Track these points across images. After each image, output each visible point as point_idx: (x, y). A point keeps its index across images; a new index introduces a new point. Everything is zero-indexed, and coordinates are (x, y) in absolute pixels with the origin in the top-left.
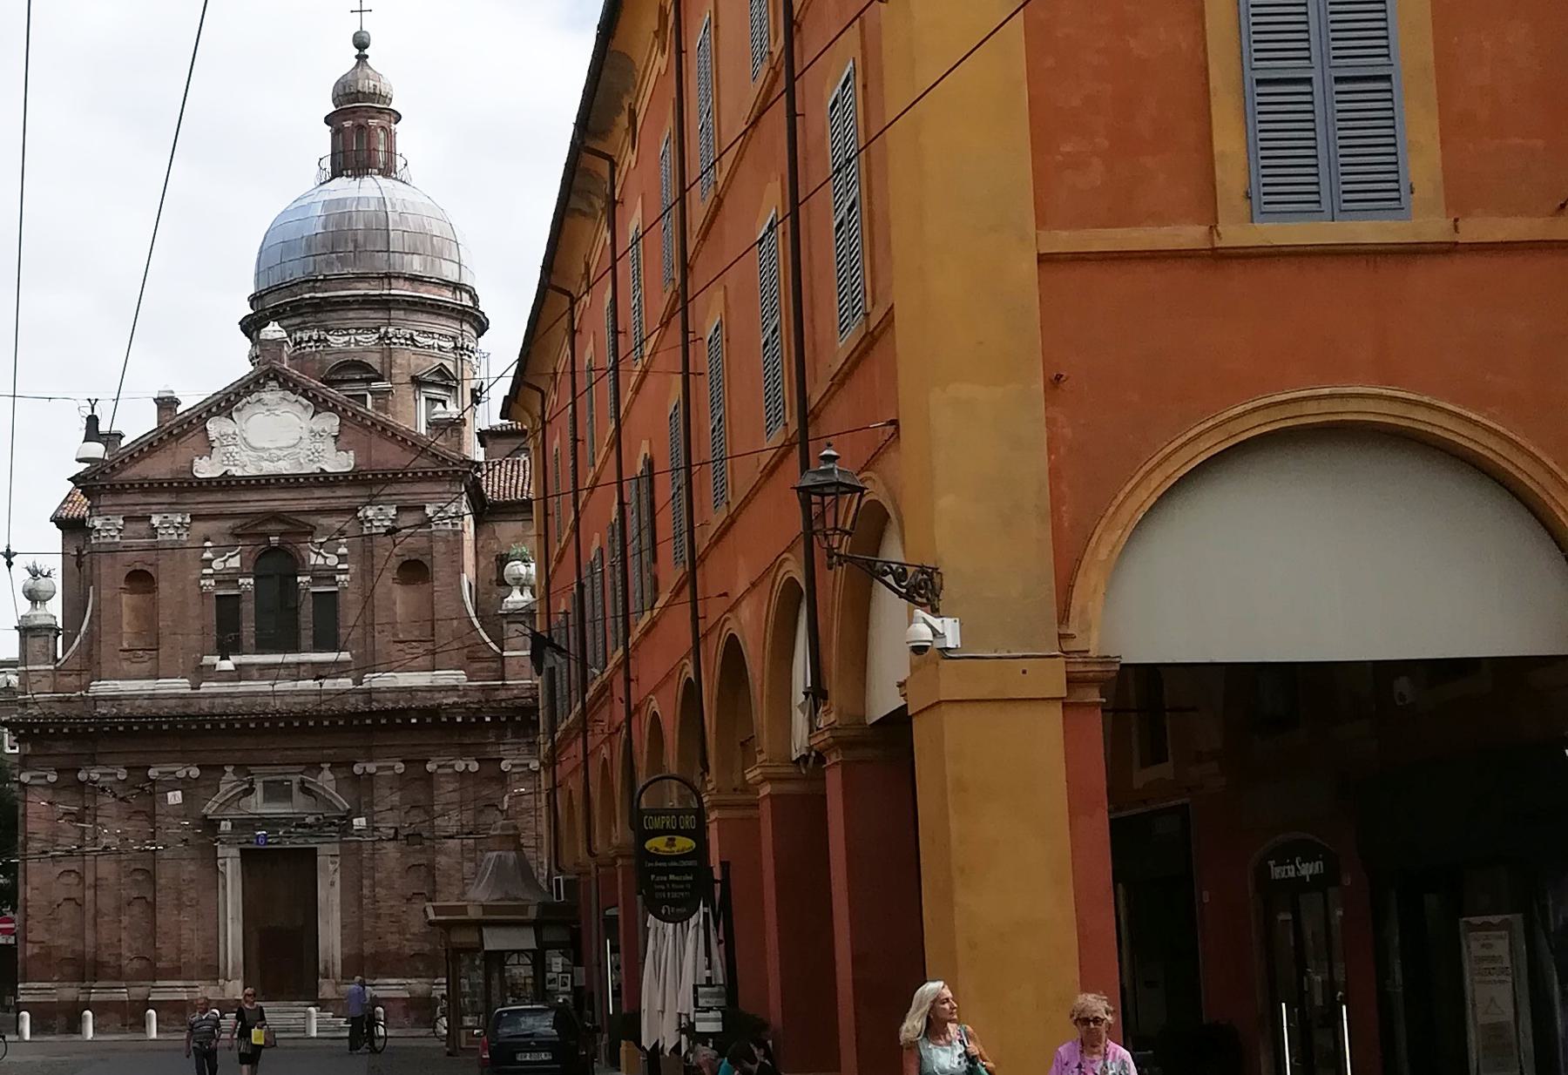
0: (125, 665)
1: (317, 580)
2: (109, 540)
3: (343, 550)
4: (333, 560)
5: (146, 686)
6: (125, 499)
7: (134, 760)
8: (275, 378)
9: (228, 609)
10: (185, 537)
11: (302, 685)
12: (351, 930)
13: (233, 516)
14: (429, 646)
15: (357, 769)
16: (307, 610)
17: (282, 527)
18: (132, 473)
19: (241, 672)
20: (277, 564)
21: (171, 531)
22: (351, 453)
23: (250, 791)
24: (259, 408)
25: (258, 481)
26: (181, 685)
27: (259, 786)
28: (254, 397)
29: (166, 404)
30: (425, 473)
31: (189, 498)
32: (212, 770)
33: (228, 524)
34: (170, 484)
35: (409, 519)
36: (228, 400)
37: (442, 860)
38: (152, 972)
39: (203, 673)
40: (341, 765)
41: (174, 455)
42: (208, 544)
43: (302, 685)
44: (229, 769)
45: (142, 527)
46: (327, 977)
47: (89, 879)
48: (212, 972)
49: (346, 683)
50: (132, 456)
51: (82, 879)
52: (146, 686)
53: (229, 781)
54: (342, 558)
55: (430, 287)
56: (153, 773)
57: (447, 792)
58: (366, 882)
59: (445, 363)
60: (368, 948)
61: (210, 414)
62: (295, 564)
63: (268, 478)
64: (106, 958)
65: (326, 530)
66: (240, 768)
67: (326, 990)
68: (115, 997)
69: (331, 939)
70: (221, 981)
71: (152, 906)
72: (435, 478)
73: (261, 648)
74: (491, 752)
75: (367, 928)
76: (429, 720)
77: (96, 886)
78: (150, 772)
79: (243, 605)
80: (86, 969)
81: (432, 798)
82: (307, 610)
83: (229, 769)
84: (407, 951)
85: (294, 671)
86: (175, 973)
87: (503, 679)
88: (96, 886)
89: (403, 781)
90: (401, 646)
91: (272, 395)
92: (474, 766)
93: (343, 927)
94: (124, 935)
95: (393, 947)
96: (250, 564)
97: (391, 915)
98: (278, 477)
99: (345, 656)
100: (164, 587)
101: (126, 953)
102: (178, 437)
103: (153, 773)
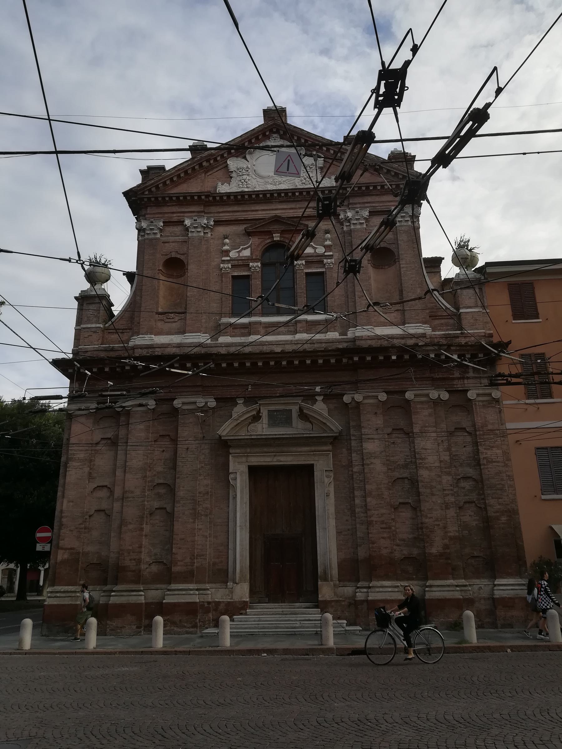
0: (160, 325)
1: (309, 263)
3: (328, 243)
4: (321, 250)
5: (176, 339)
7: (162, 393)
8: (277, 132)
9: (241, 283)
10: (209, 235)
11: (299, 336)
12: (348, 537)
13: (246, 221)
15: (346, 399)
16: (301, 283)
17: (283, 228)
19: (248, 329)
20: (279, 256)
23: (257, 418)
25: (265, 195)
26: (203, 338)
27: (264, 413)
31: (213, 209)
33: (241, 228)
34: (199, 197)
37: (424, 473)
38: (167, 576)
39: (219, 330)
44: (240, 401)
45: (178, 229)
46: (325, 579)
47: (118, 492)
48: (222, 575)
49: (333, 335)
50: (171, 179)
51: (112, 492)
52: (176, 339)
53: (240, 410)
54: (328, 248)
56: (177, 403)
57: (423, 417)
58: (357, 493)
60: (362, 553)
63: (272, 192)
66: (250, 400)
67: (326, 592)
68: (133, 599)
69: (328, 547)
70: (230, 584)
71: (170, 516)
73: (263, 314)
74: (458, 385)
75: (359, 534)
77: (123, 499)
78: (175, 402)
79: (253, 282)
80: (109, 573)
81: (411, 424)
82: (301, 283)
83: (240, 401)
84: (398, 555)
85: (292, 329)
86: (188, 576)
87: (461, 328)
88: (123, 499)
89: (385, 408)
92: (445, 396)
93: (339, 533)
94: (145, 542)
95: (385, 552)
96: (258, 254)
97: (383, 522)
98: (279, 192)
100: (192, 269)
101: (145, 557)
103: (177, 403)
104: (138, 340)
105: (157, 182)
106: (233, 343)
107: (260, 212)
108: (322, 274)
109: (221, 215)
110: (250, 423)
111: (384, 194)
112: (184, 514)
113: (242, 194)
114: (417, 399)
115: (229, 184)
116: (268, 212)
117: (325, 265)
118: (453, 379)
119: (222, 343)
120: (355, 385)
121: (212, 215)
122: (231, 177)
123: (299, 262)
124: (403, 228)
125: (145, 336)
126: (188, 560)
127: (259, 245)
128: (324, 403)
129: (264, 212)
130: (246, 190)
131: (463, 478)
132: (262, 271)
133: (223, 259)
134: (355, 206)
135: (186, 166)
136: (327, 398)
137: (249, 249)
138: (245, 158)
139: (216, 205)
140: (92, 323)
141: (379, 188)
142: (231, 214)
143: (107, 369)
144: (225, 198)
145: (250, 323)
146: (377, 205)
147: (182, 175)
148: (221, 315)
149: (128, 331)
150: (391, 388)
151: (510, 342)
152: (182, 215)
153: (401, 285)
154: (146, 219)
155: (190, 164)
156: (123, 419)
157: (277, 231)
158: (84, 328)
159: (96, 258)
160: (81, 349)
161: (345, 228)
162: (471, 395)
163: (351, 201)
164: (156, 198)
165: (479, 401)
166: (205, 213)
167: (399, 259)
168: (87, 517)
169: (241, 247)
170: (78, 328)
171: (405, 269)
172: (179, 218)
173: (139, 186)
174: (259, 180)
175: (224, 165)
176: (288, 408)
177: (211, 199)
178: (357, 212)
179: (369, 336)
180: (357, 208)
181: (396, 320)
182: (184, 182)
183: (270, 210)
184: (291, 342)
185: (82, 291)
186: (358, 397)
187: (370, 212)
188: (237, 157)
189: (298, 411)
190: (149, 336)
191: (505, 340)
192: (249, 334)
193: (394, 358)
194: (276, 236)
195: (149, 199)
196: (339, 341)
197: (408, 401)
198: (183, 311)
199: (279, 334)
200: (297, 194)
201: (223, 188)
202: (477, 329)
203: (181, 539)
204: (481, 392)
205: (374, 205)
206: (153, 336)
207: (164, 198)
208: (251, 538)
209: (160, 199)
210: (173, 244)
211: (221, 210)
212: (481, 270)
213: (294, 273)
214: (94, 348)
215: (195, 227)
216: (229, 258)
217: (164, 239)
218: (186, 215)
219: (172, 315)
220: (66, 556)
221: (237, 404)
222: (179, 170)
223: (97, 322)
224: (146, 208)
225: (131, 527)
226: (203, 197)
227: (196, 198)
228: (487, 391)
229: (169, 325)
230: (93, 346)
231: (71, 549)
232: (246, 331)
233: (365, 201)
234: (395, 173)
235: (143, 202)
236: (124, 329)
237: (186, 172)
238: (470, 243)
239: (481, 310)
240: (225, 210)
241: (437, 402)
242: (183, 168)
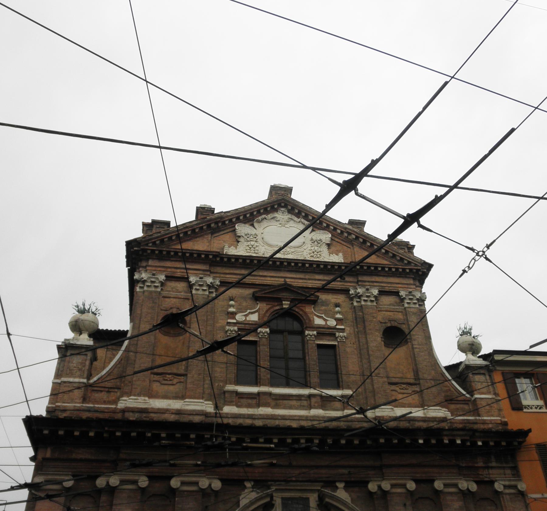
0: (156, 386)
2: (153, 289)
3: (339, 316)
4: (332, 323)
8: (285, 206)
14: (417, 389)
15: (372, 487)
16: (313, 356)
19: (257, 399)
21: (205, 288)
22: (341, 255)
24: (273, 222)
28: (270, 216)
31: (219, 269)
32: (234, 484)
33: (248, 292)
34: (207, 256)
35: (387, 300)
36: (252, 214)
40: (355, 484)
41: (210, 242)
42: (232, 303)
43: (314, 412)
44: (248, 485)
45: (181, 286)
52: (176, 405)
56: (175, 483)
61: (238, 220)
62: (303, 323)
65: (326, 303)
66: (260, 484)
73: (272, 385)
74: (485, 475)
76: (433, 441)
82: (313, 356)
83: (248, 485)
85: (305, 403)
90: (393, 387)
91: (282, 215)
92: (474, 487)
99: (349, 392)
103: (175, 483)
104: (128, 402)
105: (163, 235)
106: (240, 415)
107: (269, 279)
108: (334, 347)
109: (228, 276)
111: (391, 276)
113: (251, 258)
114: (447, 490)
115: (236, 248)
116: (277, 279)
117: (337, 338)
118: (478, 468)
119: (227, 414)
120: (381, 471)
121: (218, 275)
122: (238, 242)
123: (311, 333)
124: (412, 310)
125: (139, 398)
127: (267, 311)
128: (346, 491)
129: (272, 279)
130: (254, 255)
132: (269, 337)
133: (229, 321)
134: (364, 284)
135: (194, 225)
136: (349, 485)
137: (257, 314)
138: (252, 225)
139: (223, 266)
140: (75, 377)
143: (92, 434)
144: (233, 260)
145: (259, 394)
146: (385, 285)
147: (189, 233)
148: (227, 382)
149: (116, 390)
150: (418, 476)
151: (530, 431)
153: (416, 365)
154: (146, 271)
156: (104, 498)
157: (287, 298)
158: (65, 382)
159: (84, 305)
160: (59, 406)
161: (355, 304)
162: (498, 486)
163: (360, 279)
164: (161, 252)
165: (506, 494)
166: (211, 272)
167: (411, 339)
169: (248, 311)
170: (58, 381)
172: (183, 274)
173: (142, 237)
174: (267, 247)
175: (231, 229)
176: (305, 495)
177: (218, 259)
178: (367, 290)
179: (390, 417)
180: (367, 285)
182: (190, 240)
183: (279, 277)
184: (307, 418)
185: (66, 340)
186: (386, 485)
187: (379, 291)
188: (245, 223)
189: (317, 499)
190: (143, 398)
191: (526, 428)
192: (258, 405)
193: (421, 441)
194: (285, 304)
195: (153, 251)
197: (437, 492)
198: (182, 371)
199: (291, 408)
200: (307, 265)
201: (232, 251)
202: (492, 416)
204: (507, 483)
205: (382, 285)
206: (147, 398)
207: (169, 252)
209: (164, 253)
210: (175, 300)
211: (228, 271)
212: (485, 357)
213: (304, 343)
214: (75, 406)
215: (201, 285)
216: (235, 321)
217: (164, 293)
219: (170, 376)
221: (245, 487)
222: (187, 227)
223: (81, 377)
224: (147, 260)
226: (211, 257)
227: (203, 256)
228: (513, 483)
229: (166, 387)
230: (73, 404)
232: (254, 402)
233: (373, 280)
234: (401, 258)
235: (145, 254)
236: (111, 388)
237: (193, 231)
238: (472, 331)
239: (494, 396)
240: (232, 272)
241: (466, 494)
242: (192, 226)
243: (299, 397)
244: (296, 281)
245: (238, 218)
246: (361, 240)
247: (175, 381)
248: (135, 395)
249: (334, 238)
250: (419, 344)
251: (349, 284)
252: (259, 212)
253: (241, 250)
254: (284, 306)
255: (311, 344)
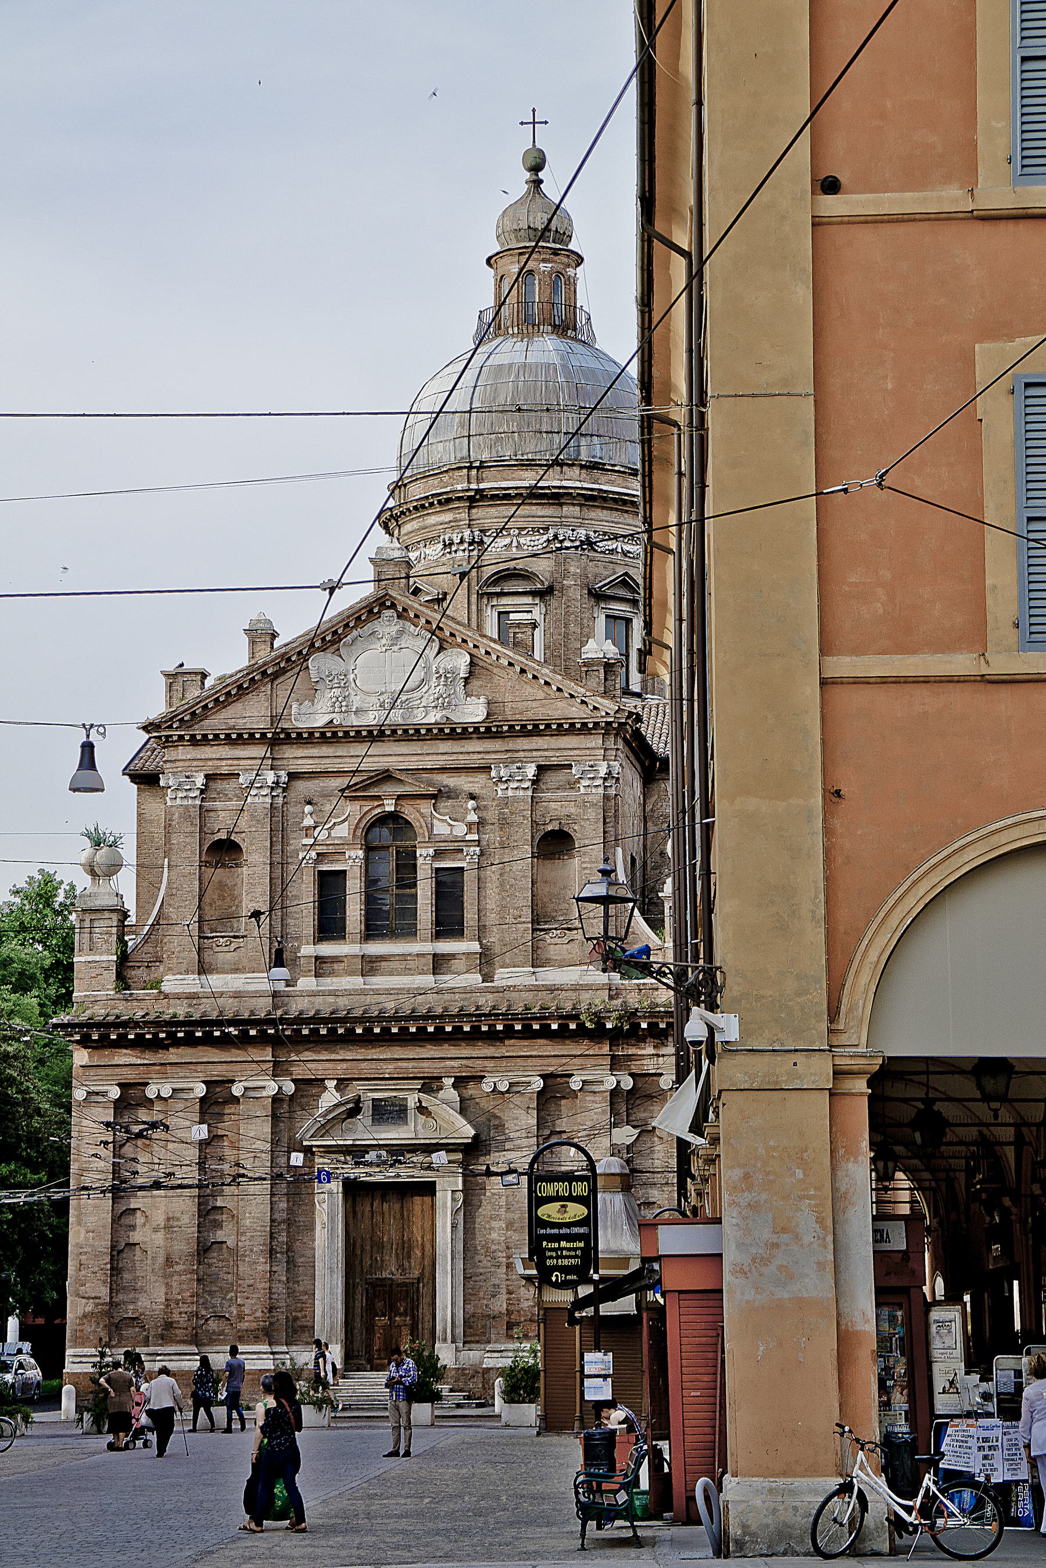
3: (473, 817)
4: (460, 829)
6: (207, 752)
10: (280, 800)
18: (217, 722)
28: (368, 628)
29: (261, 634)
30: (572, 725)
36: (335, 633)
42: (308, 809)
46: (445, 1340)
55: (614, 477)
59: (631, 572)
64: (176, 1317)
72: (584, 729)
83: (331, 1084)
102: (276, 676)
109: (300, 762)
110: (345, 1119)
112: (252, 1251)
123: (424, 852)
126: (259, 1314)
131: (644, 1203)
141: (554, 727)
142: (317, 761)
146: (550, 754)
152: (235, 762)
155: (248, 674)
161: (500, 792)
164: (193, 736)
168: (115, 1253)
171: (588, 872)
181: (570, 956)
190: (192, 977)
195: (181, 738)
196: (481, 991)
203: (249, 1286)
205: (546, 754)
208: (347, 1283)
218: (242, 762)
220: (89, 1309)
225: (178, 1268)
231: (96, 1298)
233: (534, 746)
243: (404, 957)
244: (408, 758)
245: (312, 645)
246: (518, 669)
247: (233, 946)
248: (181, 974)
249: (476, 660)
250: (591, 862)
251: (494, 756)
252: (347, 625)
253: (317, 716)
254: (387, 809)
255: (424, 870)
